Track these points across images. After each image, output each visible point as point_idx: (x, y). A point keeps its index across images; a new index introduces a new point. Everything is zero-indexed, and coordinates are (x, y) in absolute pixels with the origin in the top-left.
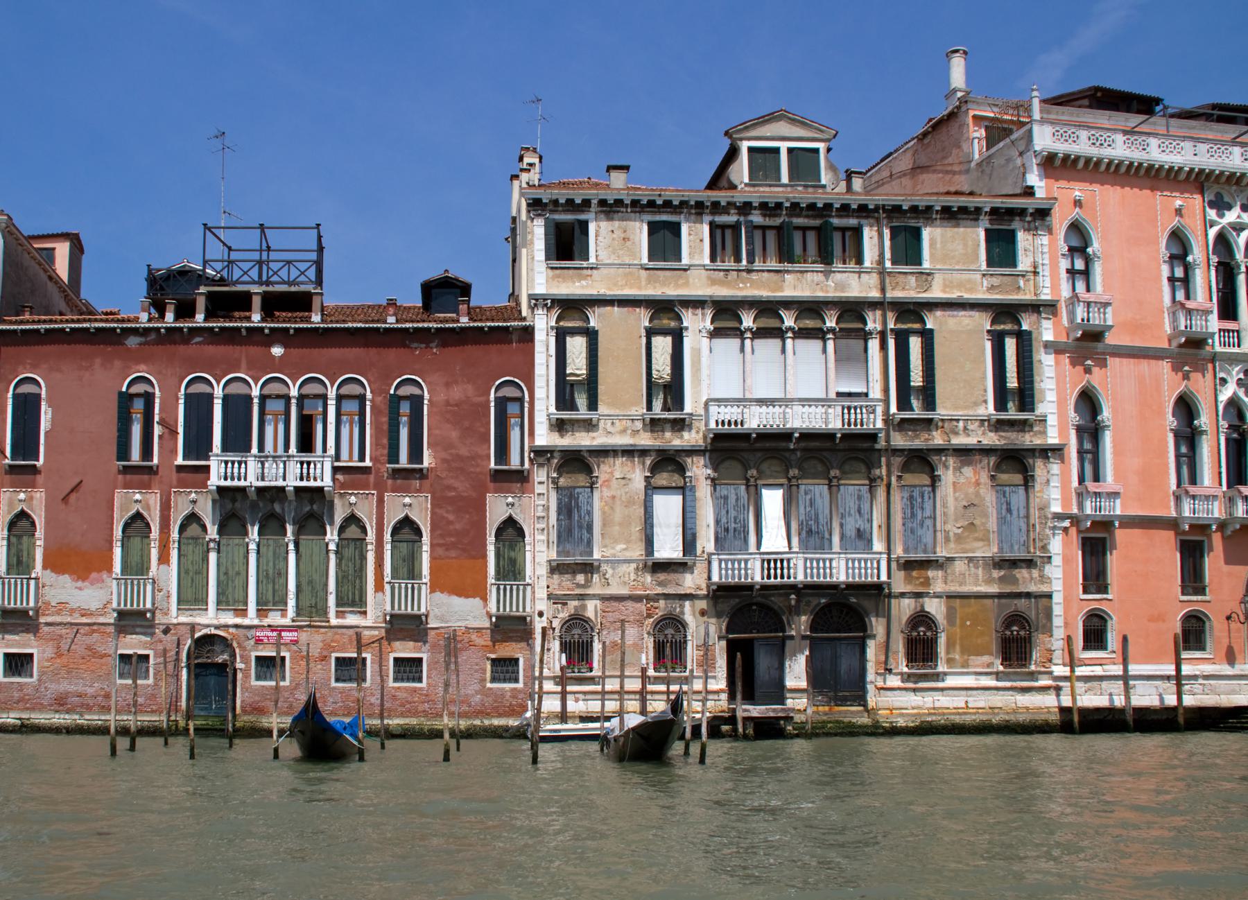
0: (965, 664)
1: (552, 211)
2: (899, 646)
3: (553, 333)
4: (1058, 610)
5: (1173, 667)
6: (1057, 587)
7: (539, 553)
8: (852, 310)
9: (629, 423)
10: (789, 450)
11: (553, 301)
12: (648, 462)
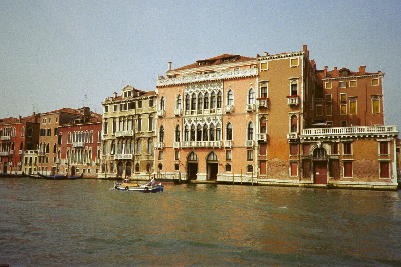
0: (142, 172)
2: (135, 169)
4: (154, 163)
7: (101, 154)
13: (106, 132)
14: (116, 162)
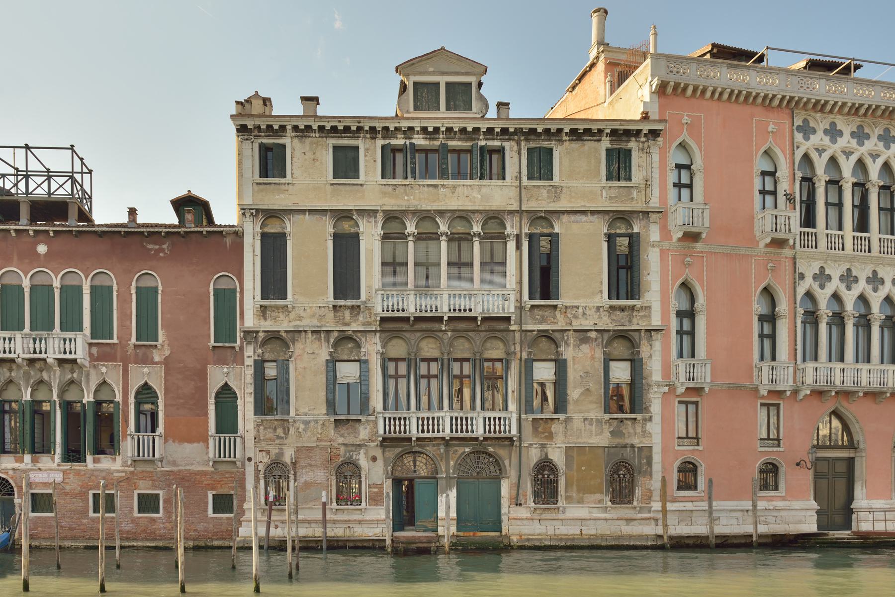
0: (580, 501)
1: (256, 136)
2: (528, 487)
3: (259, 237)
4: (657, 458)
5: (751, 503)
6: (656, 442)
8: (494, 217)
9: (317, 310)
10: (442, 331)
11: (257, 210)
12: (332, 341)
13: (274, 283)
14: (378, 453)
